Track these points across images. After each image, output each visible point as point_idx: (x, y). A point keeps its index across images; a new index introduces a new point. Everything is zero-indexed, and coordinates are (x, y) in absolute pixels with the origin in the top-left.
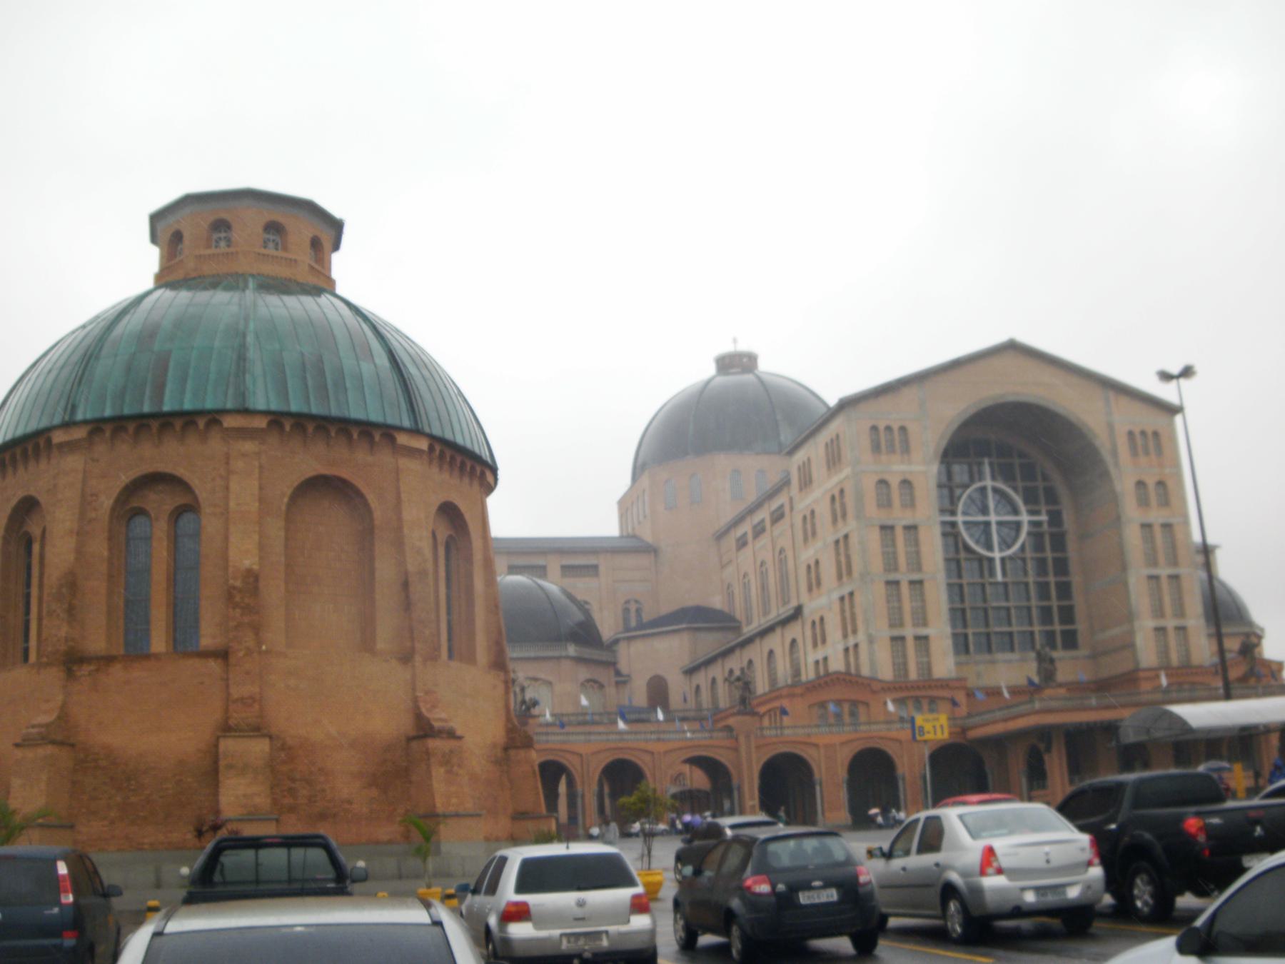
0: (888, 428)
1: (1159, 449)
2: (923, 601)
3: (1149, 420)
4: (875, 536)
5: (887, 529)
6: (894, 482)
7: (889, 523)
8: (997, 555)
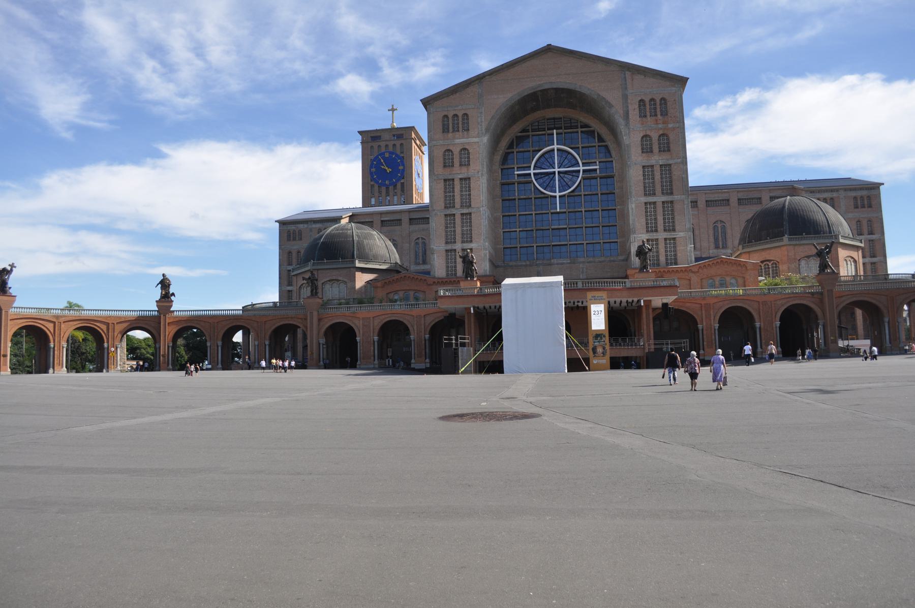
0: (456, 116)
1: (665, 113)
2: (471, 226)
3: (657, 90)
4: (441, 185)
5: (448, 182)
6: (456, 151)
7: (450, 177)
8: (558, 194)
